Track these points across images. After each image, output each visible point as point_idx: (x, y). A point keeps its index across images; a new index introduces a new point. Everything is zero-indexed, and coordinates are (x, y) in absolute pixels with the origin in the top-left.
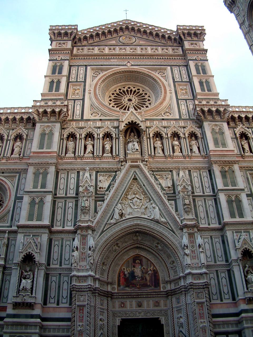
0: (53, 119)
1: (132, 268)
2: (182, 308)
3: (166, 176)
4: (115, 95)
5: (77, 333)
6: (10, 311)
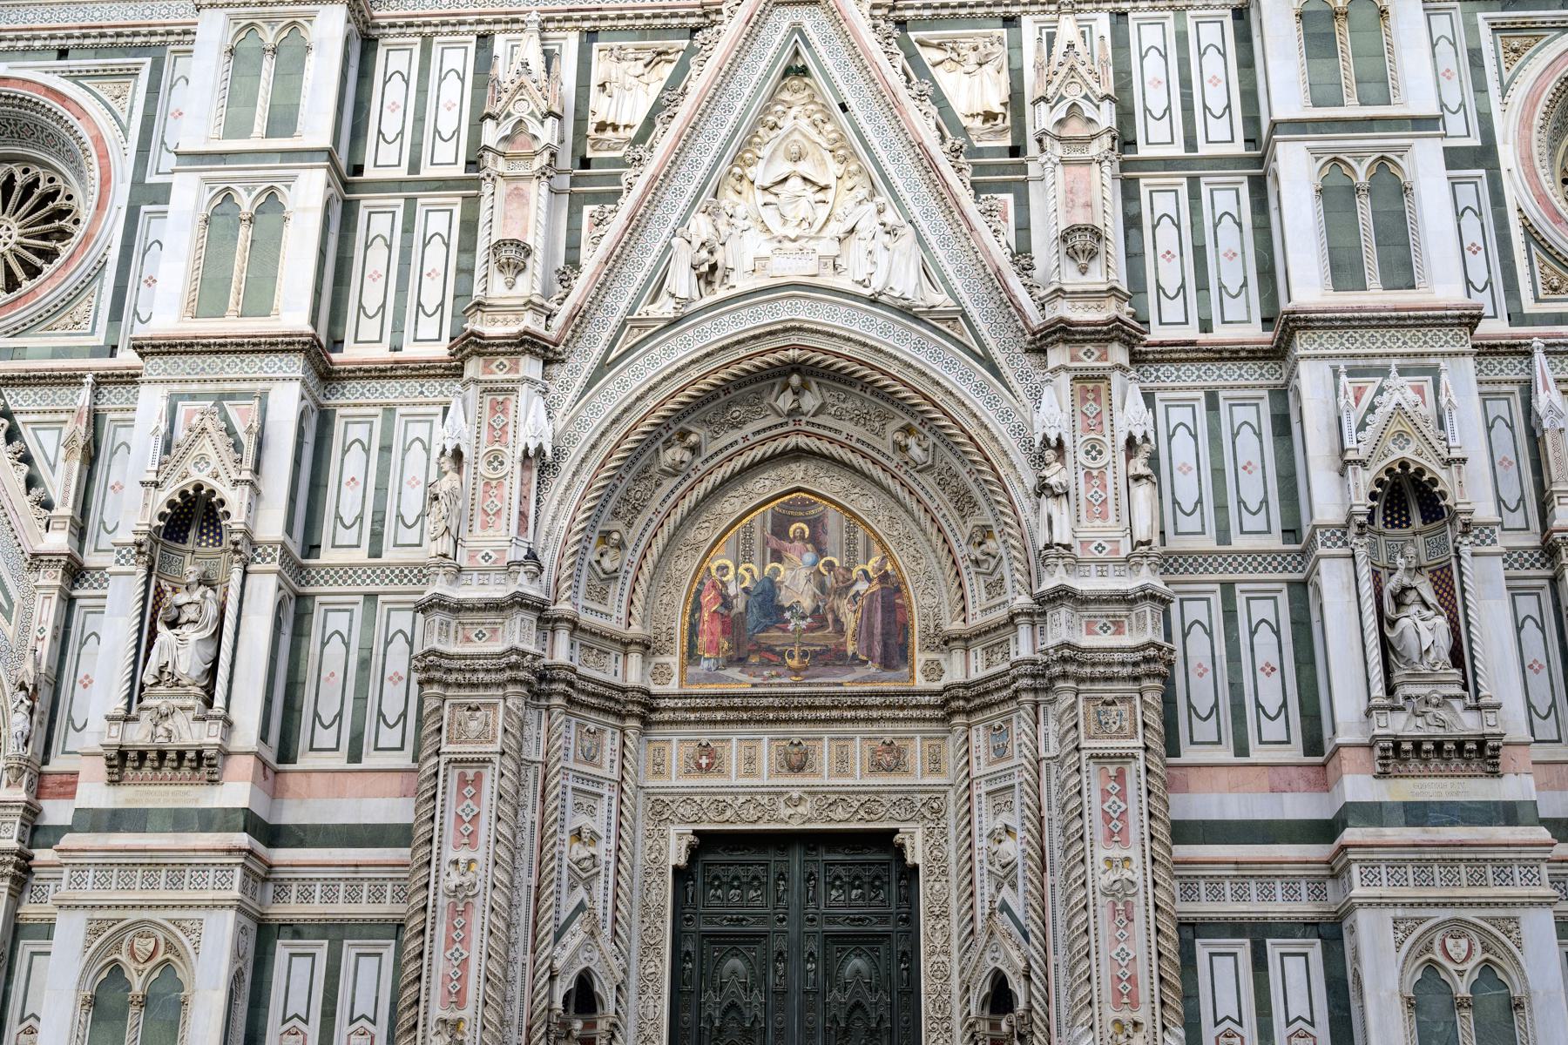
1: (764, 565)
2: (1016, 781)
3: (975, 49)
5: (443, 902)
6: (95, 793)
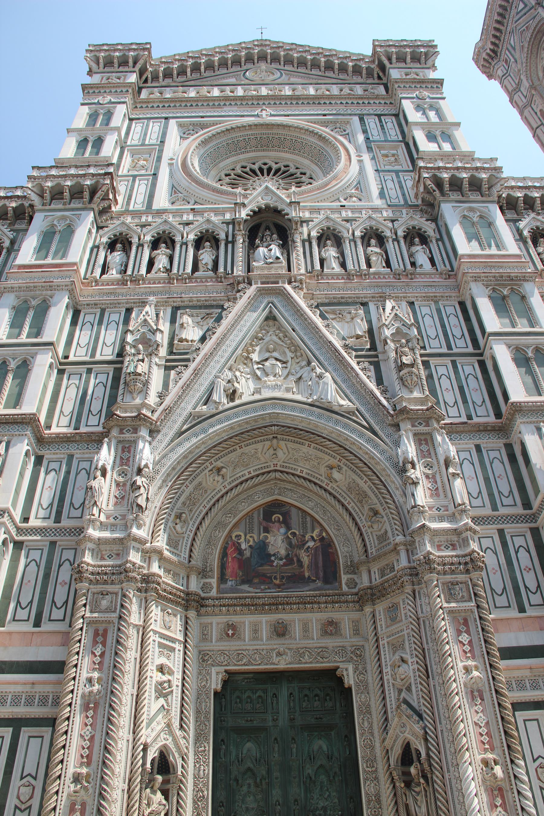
0: (75, 204)
1: (260, 534)
3: (350, 313)
4: (233, 176)
